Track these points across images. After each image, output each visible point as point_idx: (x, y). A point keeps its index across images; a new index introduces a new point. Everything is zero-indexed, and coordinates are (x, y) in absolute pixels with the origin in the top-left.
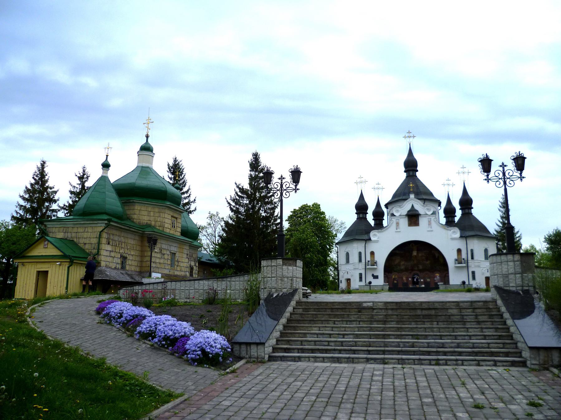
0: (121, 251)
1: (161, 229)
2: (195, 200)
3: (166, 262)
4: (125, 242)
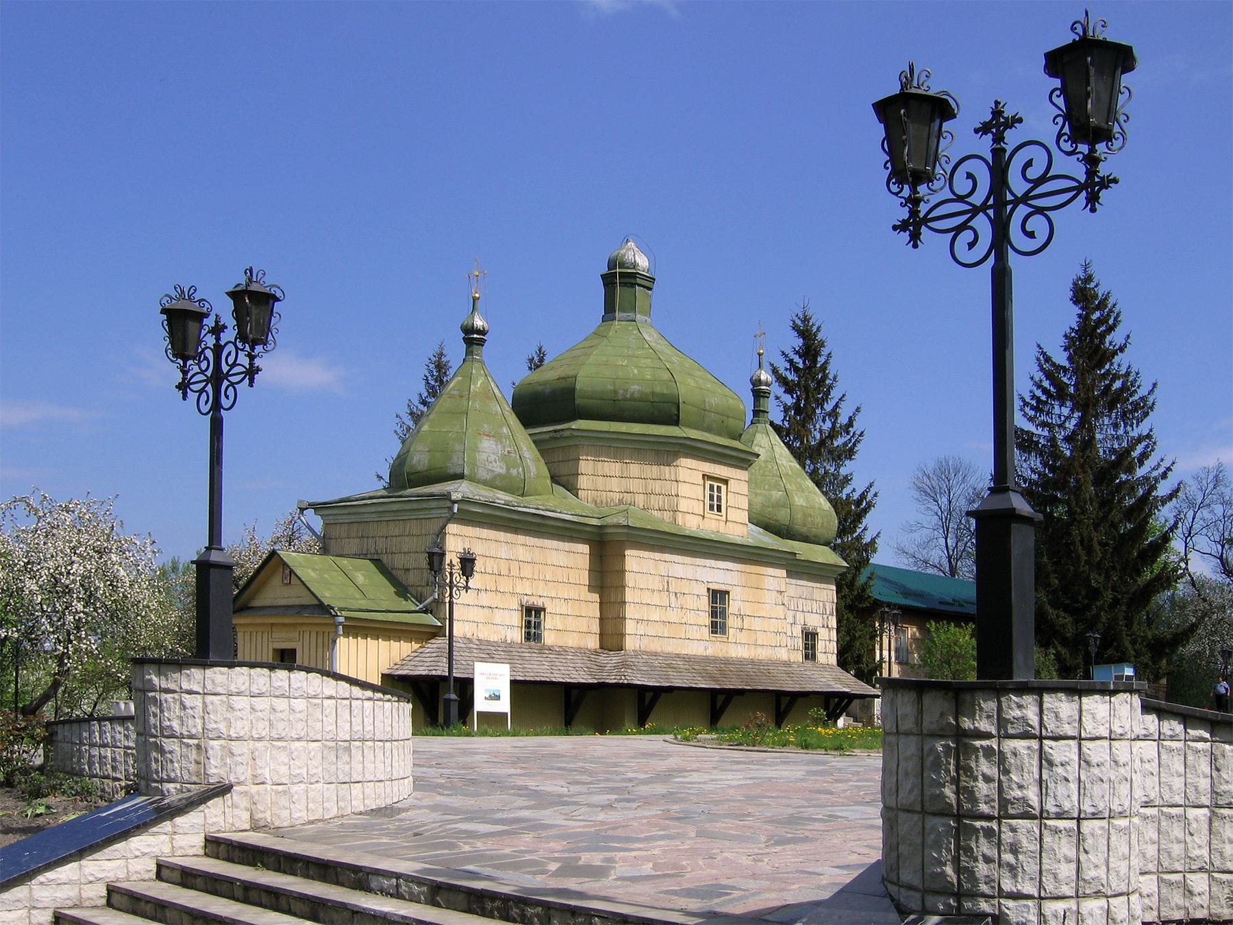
1: (667, 516)
3: (690, 617)
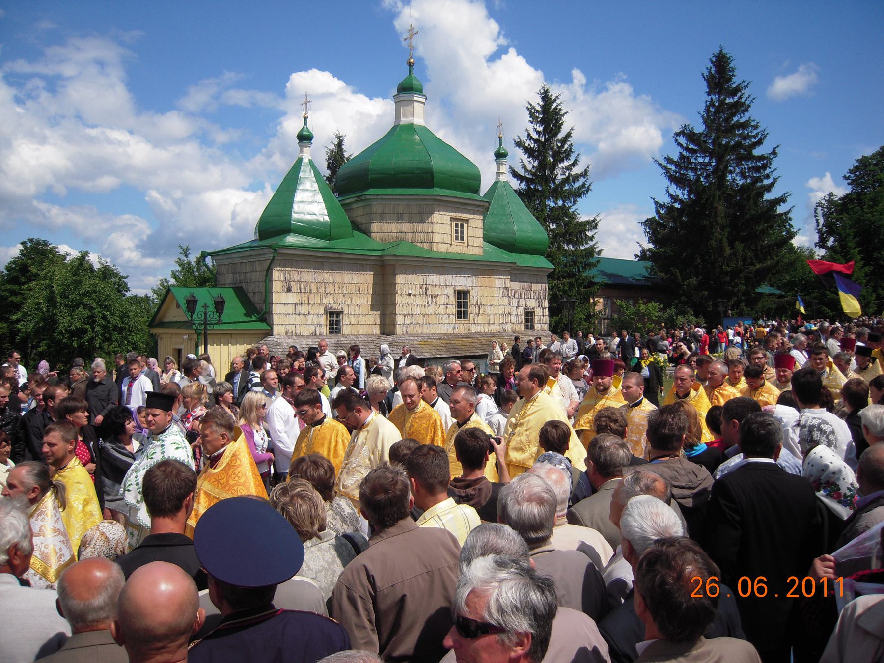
0: (325, 301)
1: (426, 246)
2: (586, 171)
3: (442, 310)
4: (334, 283)
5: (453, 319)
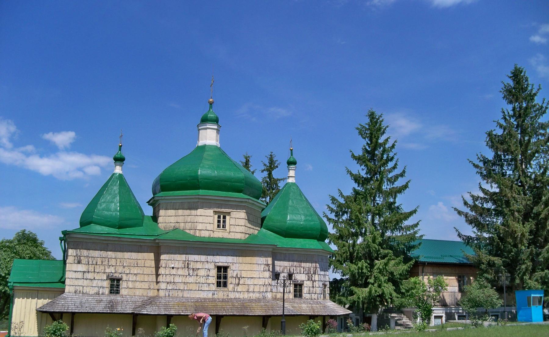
0: (108, 271)
1: (192, 232)
3: (202, 280)
5: (214, 287)
